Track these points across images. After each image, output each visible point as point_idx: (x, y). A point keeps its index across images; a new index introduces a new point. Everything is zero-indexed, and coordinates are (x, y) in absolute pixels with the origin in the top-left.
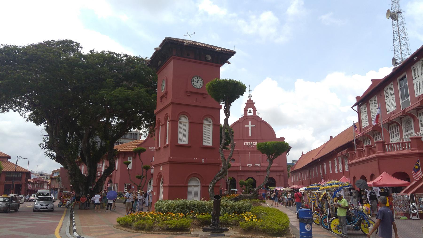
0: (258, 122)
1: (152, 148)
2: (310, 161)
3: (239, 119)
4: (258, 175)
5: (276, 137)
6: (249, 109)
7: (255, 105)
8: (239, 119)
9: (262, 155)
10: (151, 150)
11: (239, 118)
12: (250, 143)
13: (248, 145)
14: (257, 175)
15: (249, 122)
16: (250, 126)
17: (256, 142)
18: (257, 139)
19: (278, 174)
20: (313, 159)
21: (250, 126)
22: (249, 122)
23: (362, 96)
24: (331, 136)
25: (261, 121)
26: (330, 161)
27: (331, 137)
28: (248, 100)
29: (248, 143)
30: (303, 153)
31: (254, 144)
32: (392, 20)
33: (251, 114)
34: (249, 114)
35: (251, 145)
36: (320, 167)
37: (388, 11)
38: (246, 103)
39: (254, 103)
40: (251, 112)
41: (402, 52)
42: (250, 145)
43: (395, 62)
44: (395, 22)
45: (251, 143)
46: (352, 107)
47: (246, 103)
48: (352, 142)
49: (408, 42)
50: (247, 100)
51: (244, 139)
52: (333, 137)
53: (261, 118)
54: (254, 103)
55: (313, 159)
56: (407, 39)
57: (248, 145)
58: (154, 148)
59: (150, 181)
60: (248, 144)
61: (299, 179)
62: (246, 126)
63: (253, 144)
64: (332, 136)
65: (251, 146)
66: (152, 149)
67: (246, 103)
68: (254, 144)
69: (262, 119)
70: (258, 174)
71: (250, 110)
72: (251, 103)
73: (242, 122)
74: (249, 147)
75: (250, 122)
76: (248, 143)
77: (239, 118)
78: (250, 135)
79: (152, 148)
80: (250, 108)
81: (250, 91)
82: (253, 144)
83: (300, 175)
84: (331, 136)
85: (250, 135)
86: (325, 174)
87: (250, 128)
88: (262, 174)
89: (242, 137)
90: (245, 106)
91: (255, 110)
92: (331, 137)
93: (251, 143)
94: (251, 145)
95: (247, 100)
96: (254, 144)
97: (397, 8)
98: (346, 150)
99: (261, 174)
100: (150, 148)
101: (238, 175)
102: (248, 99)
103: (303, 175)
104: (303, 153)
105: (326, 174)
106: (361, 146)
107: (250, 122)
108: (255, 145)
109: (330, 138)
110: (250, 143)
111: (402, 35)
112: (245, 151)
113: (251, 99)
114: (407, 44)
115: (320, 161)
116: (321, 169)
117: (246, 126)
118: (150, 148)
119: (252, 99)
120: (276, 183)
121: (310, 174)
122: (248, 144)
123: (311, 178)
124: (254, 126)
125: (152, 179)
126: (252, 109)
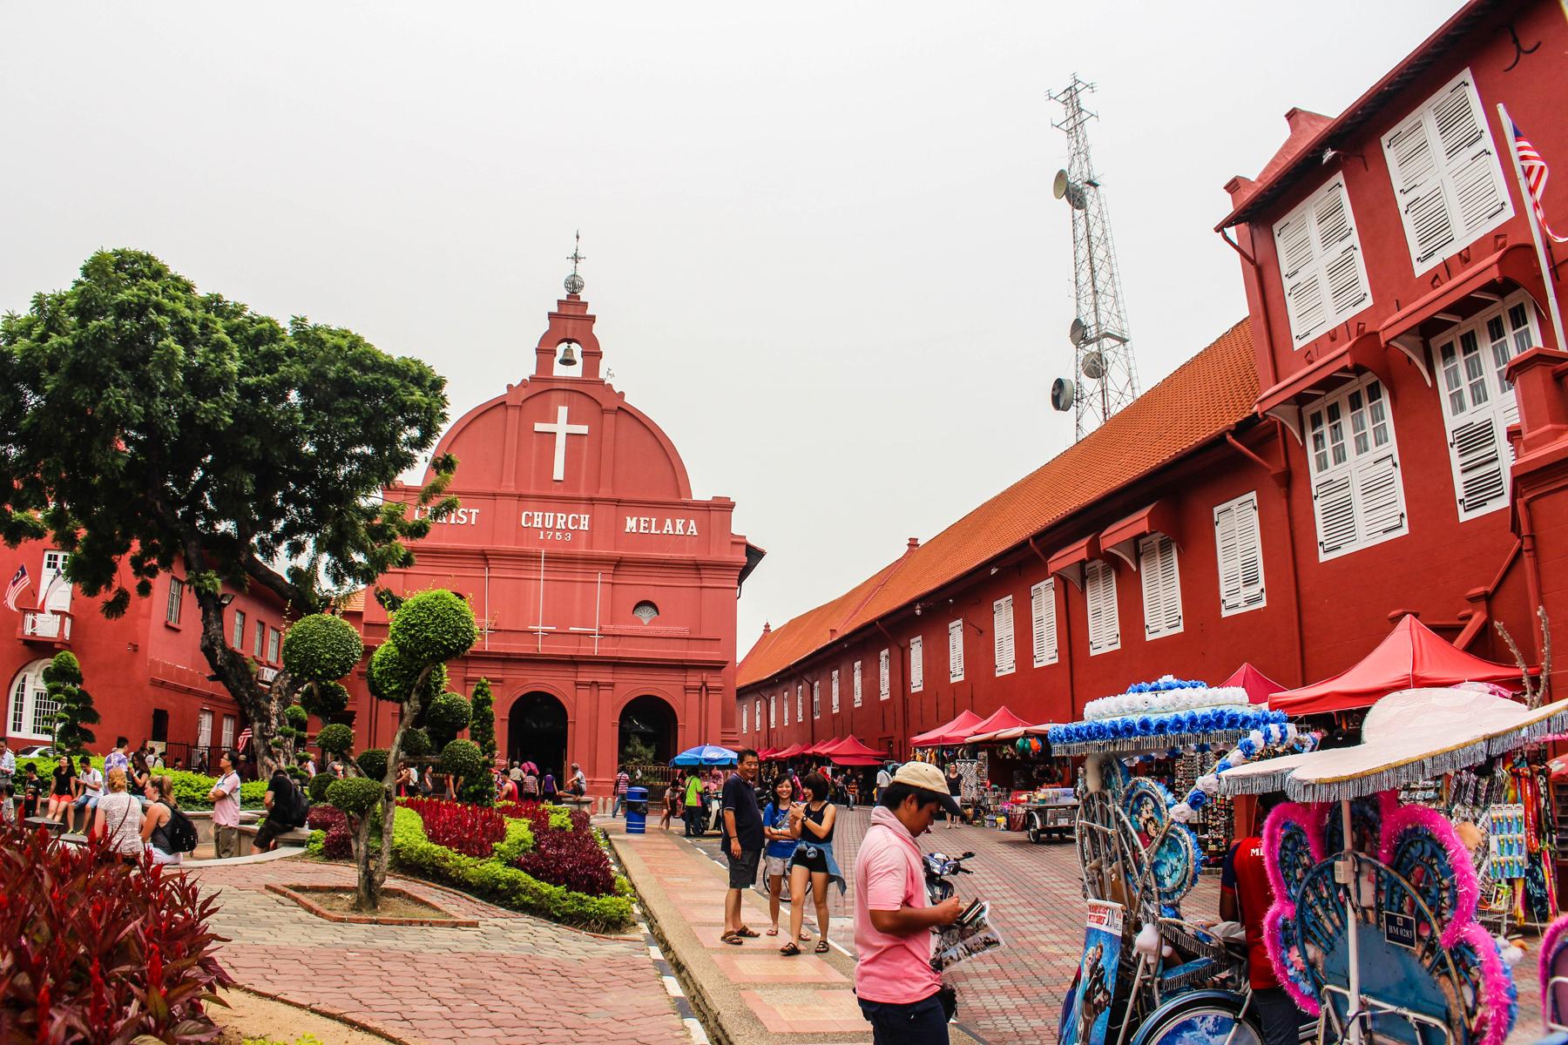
0: (603, 411)
2: (825, 640)
3: (505, 392)
4: (579, 679)
5: (689, 494)
6: (561, 349)
7: (597, 330)
8: (505, 392)
9: (613, 584)
11: (510, 387)
12: (555, 518)
13: (540, 526)
14: (577, 684)
15: (560, 408)
16: (562, 426)
17: (587, 516)
18: (591, 499)
19: (694, 679)
20: (833, 631)
21: (562, 426)
22: (560, 408)
23: (1259, 180)
28: (565, 298)
29: (544, 516)
30: (767, 626)
32: (1071, 207)
34: (560, 371)
35: (558, 527)
36: (883, 659)
37: (1061, 175)
39: (592, 319)
41: (1101, 307)
42: (554, 529)
43: (1079, 334)
44: (1078, 213)
46: (1220, 229)
48: (1229, 437)
49: (1116, 278)
50: (560, 302)
51: (520, 496)
52: (921, 542)
53: (622, 394)
54: (592, 319)
55: (833, 631)
56: (1115, 271)
61: (872, 688)
62: (539, 427)
63: (566, 523)
65: (558, 534)
67: (551, 316)
70: (586, 676)
71: (568, 351)
72: (575, 317)
73: (521, 407)
74: (545, 535)
75: (563, 412)
76: (544, 516)
77: (510, 387)
78: (559, 473)
80: (570, 341)
81: (576, 258)
82: (566, 523)
83: (758, 709)
85: (559, 473)
86: (913, 690)
88: (603, 676)
89: (513, 484)
91: (593, 355)
92: (913, 543)
93: (559, 515)
94: (558, 527)
95: (560, 302)
96: (576, 522)
97: (1085, 170)
98: (1145, 512)
99: (599, 680)
101: (469, 675)
102: (563, 296)
104: (767, 626)
106: (1284, 464)
107: (563, 412)
109: (907, 548)
110: (555, 518)
111: (1099, 253)
112: (523, 558)
113: (579, 297)
114: (1114, 285)
115: (918, 612)
116: (885, 673)
117: (539, 427)
119: (584, 296)
120: (680, 731)
122: (537, 518)
123: (817, 717)
124: (584, 429)
126: (577, 349)
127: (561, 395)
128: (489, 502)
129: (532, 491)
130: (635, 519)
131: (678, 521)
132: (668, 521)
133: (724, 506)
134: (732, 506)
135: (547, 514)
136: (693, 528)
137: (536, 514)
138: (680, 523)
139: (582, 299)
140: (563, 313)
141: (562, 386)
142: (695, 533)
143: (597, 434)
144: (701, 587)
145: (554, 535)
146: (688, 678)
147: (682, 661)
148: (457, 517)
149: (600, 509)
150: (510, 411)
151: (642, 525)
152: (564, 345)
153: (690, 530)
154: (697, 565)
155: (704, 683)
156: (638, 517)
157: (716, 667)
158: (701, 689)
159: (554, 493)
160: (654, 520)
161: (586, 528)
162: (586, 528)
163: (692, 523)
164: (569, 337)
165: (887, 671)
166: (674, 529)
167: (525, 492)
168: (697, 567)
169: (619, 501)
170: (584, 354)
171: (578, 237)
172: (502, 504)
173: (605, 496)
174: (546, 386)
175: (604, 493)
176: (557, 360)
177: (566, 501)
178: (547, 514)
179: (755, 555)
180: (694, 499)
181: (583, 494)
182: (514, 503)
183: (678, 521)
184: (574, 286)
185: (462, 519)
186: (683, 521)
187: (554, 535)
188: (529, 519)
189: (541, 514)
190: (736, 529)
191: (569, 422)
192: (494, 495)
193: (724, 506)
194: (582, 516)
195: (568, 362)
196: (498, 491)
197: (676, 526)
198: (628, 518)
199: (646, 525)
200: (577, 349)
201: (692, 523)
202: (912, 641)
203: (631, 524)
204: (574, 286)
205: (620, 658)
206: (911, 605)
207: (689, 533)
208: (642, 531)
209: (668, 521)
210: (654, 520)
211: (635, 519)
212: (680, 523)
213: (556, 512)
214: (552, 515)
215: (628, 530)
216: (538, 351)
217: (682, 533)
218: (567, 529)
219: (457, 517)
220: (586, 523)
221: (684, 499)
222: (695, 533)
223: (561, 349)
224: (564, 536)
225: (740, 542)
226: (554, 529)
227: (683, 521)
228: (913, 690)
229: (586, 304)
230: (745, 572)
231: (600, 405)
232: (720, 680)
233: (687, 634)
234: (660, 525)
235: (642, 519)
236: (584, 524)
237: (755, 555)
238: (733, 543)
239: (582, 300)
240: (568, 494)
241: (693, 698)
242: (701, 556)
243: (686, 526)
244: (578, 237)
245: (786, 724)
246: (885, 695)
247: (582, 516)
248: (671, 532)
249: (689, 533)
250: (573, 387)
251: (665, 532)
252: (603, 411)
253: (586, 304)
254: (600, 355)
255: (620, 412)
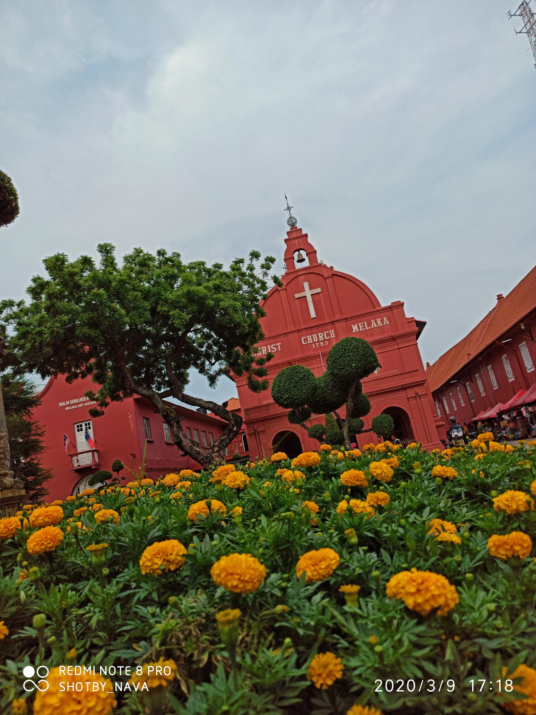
0: (325, 279)
1: (68, 403)
5: (380, 306)
6: (296, 255)
7: (310, 240)
10: (67, 408)
12: (318, 336)
13: (311, 342)
17: (333, 331)
18: (332, 322)
19: (411, 393)
20: (469, 355)
21: (308, 293)
24: (498, 296)
25: (333, 274)
26: (490, 366)
27: (500, 297)
29: (312, 337)
31: (328, 335)
33: (306, 263)
34: (298, 266)
35: (320, 340)
38: (286, 241)
39: (306, 235)
40: (303, 260)
42: (319, 341)
45: (319, 334)
47: (286, 241)
50: (288, 233)
51: (298, 331)
52: (505, 295)
53: (332, 268)
54: (306, 235)
55: (469, 355)
57: (311, 342)
58: (72, 403)
59: (79, 490)
60: (311, 339)
63: (324, 337)
64: (502, 295)
65: (321, 343)
66: (67, 406)
68: (327, 337)
69: (335, 269)
71: (300, 255)
74: (316, 346)
75: (306, 285)
76: (312, 337)
78: (313, 314)
79: (68, 403)
81: (289, 208)
82: (324, 337)
84: (498, 296)
85: (313, 314)
87: (309, 299)
90: (285, 247)
91: (312, 253)
92: (500, 297)
93: (319, 334)
94: (320, 340)
95: (288, 233)
100: (61, 404)
103: (445, 402)
105: (484, 394)
107: (306, 285)
108: (332, 337)
109: (497, 301)
110: (318, 336)
113: (296, 227)
115: (523, 327)
117: (297, 296)
118: (61, 404)
119: (298, 226)
121: (469, 392)
124: (319, 290)
125: (81, 484)
126: (303, 253)
127: (303, 277)
128: (284, 338)
129: (303, 327)
130: (356, 325)
131: (378, 320)
132: (373, 321)
133: (399, 305)
134: (403, 304)
135: (313, 335)
136: (386, 321)
137: (308, 337)
138: (379, 321)
139: (298, 228)
140: (291, 237)
141: (302, 273)
142: (388, 323)
143: (325, 289)
144: (399, 348)
145: (320, 345)
146: (408, 393)
147: (402, 385)
148: (271, 349)
149: (337, 325)
150: (281, 292)
151: (360, 327)
152: (297, 253)
153: (385, 322)
154: (393, 338)
155: (417, 394)
156: (358, 323)
157: (421, 384)
158: (416, 397)
159: (313, 325)
160: (365, 323)
161: (334, 336)
162: (334, 336)
163: (385, 318)
164: (298, 248)
165: (509, 366)
166: (377, 324)
167: (300, 328)
168: (394, 339)
169: (346, 319)
170: (307, 255)
171: (286, 198)
172: (290, 336)
173: (339, 319)
174: (295, 275)
175: (337, 317)
176: (295, 261)
177: (320, 327)
178: (313, 335)
179: (421, 325)
180: (382, 306)
181: (327, 321)
182: (296, 335)
183: (378, 320)
184: (292, 223)
185: (274, 350)
186: (380, 319)
187: (320, 345)
188: (306, 340)
189: (310, 336)
190: (408, 315)
191: (311, 288)
192: (286, 334)
193: (399, 305)
194: (330, 331)
195: (301, 260)
196: (287, 332)
197: (377, 323)
198: (353, 326)
199: (363, 326)
200: (303, 253)
201: (385, 318)
202: (520, 346)
203: (355, 328)
204: (292, 223)
205: (371, 392)
206: (517, 325)
207: (385, 324)
208: (361, 330)
209: (373, 321)
210: (365, 323)
211: (356, 325)
212: (379, 321)
213: (317, 333)
214: (316, 335)
215: (354, 331)
216: (285, 260)
217: (381, 325)
218: (325, 340)
219: (271, 349)
220: (333, 334)
221: (377, 309)
222: (388, 323)
223: (296, 255)
224: (324, 343)
225: (412, 320)
226: (319, 341)
227: (380, 319)
228: (529, 372)
229: (301, 230)
230: (418, 335)
231: (323, 276)
232: (424, 390)
233: (398, 373)
234: (369, 324)
235: (360, 324)
236: (333, 335)
237: (421, 325)
238: (408, 322)
239: (298, 228)
240: (321, 323)
241: (413, 402)
242: (394, 334)
243: (382, 321)
244: (286, 198)
245: (455, 409)
246: (511, 378)
247: (330, 331)
248: (376, 326)
249: (385, 324)
250: (308, 271)
251: (373, 327)
252: (325, 279)
253: (301, 230)
254: (315, 252)
255: (335, 277)
